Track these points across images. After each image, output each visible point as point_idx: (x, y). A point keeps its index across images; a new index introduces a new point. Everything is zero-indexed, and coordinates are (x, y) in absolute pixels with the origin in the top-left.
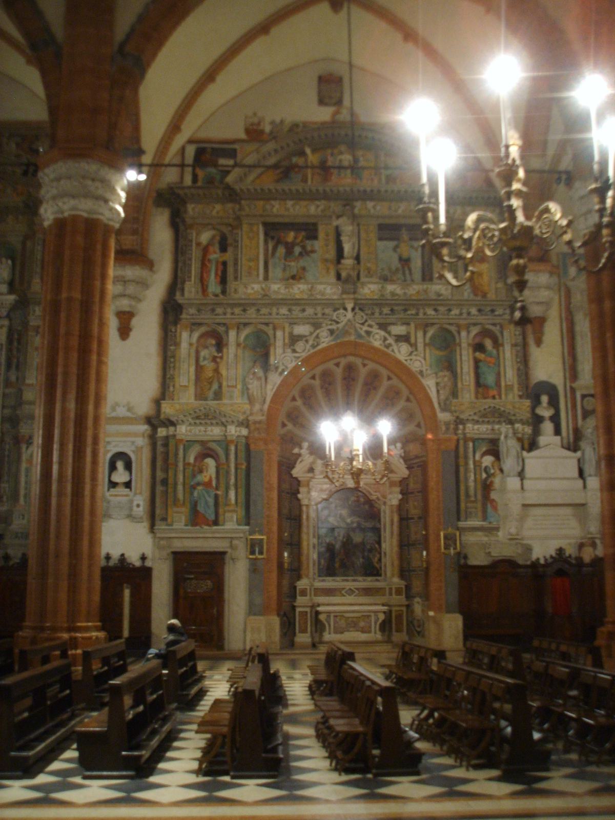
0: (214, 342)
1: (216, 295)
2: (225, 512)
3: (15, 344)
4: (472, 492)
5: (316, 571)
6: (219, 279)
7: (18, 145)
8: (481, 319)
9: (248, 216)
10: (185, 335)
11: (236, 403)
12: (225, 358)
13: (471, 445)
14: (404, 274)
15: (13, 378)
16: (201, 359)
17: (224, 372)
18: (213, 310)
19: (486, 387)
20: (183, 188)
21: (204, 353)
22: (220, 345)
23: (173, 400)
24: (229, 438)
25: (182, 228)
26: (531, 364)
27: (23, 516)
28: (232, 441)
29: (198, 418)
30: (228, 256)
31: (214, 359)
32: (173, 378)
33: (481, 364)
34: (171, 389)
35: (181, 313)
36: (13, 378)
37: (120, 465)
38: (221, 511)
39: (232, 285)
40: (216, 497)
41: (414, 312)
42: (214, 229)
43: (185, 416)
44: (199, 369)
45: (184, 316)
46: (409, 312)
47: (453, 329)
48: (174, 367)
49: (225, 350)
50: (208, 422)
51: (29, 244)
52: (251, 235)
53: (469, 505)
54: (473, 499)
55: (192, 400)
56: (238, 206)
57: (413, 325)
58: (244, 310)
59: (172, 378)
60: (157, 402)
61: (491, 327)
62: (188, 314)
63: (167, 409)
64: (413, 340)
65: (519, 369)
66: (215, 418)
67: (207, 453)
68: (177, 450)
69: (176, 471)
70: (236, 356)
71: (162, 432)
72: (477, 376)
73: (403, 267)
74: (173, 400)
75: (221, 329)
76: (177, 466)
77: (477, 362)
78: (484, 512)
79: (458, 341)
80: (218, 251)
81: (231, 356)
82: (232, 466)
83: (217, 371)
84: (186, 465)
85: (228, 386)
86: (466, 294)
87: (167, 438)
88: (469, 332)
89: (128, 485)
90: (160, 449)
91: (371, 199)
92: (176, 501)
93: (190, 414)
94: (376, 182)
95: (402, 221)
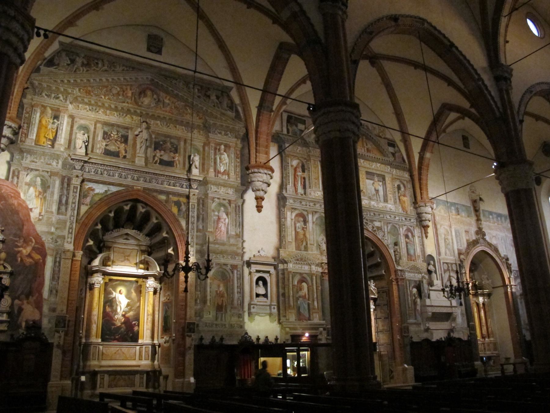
0: (302, 219)
1: (302, 195)
2: (313, 313)
3: (201, 206)
4: (410, 306)
6: (302, 186)
7: (198, 90)
8: (407, 223)
9: (312, 156)
10: (289, 214)
11: (314, 254)
12: (308, 228)
14: (377, 197)
15: (201, 227)
16: (297, 228)
17: (308, 236)
18: (301, 203)
19: (411, 256)
20: (283, 134)
21: (298, 225)
22: (305, 222)
23: (285, 249)
24: (312, 272)
25: (284, 155)
26: (425, 246)
27: (210, 312)
28: (314, 274)
29: (298, 260)
30: (306, 175)
31: (303, 229)
32: (285, 237)
33: (408, 244)
34: (284, 243)
35: (286, 202)
36: (201, 227)
37: (261, 283)
38: (311, 313)
39: (308, 190)
40: (309, 305)
42: (298, 159)
43: (291, 258)
44: (297, 233)
45: (287, 203)
47: (397, 226)
48: (285, 230)
49: (307, 225)
50: (303, 263)
51: (207, 148)
52: (315, 166)
53: (410, 312)
55: (294, 250)
56: (308, 150)
58: (315, 204)
59: (284, 236)
60: (278, 249)
61: (410, 227)
62: (289, 202)
63: (283, 253)
64: (383, 230)
65: (421, 248)
66: (305, 261)
67: (302, 280)
68: (289, 277)
69: (289, 290)
70: (313, 228)
71: (281, 266)
72: (407, 249)
74: (285, 249)
75: (305, 213)
76: (289, 286)
77: (407, 243)
78: (415, 315)
80: (301, 171)
81: (311, 228)
82: (315, 287)
83: (304, 235)
85: (311, 244)
86: (400, 210)
87: (283, 270)
88: (403, 229)
89: (265, 296)
90: (280, 276)
91: (363, 159)
92: (290, 306)
93: (294, 257)
94: (363, 150)
95: (375, 172)
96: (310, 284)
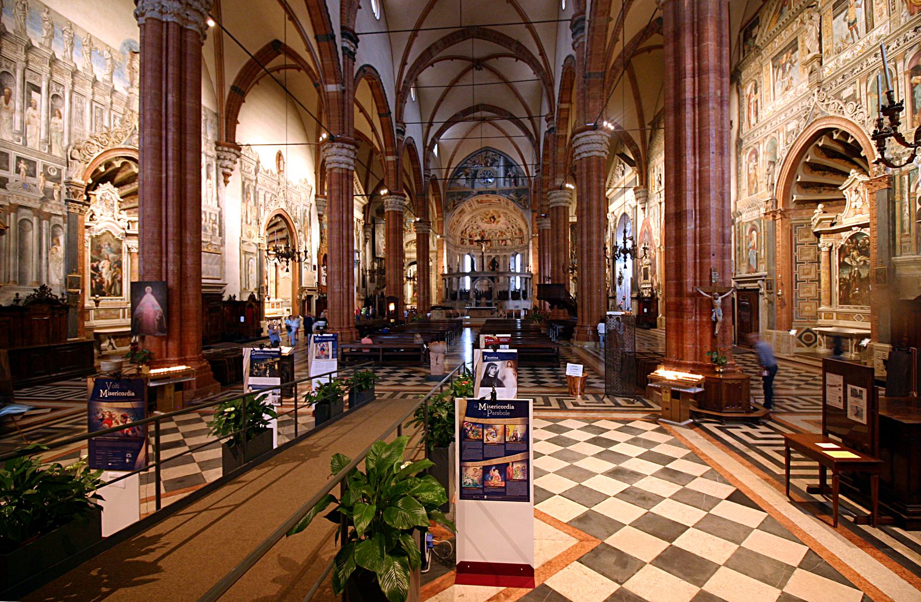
4: (906, 227)
5: (838, 300)
13: (906, 177)
14: (853, 37)
29: (749, 207)
41: (859, 69)
46: (855, 71)
53: (903, 239)
54: (907, 233)
57: (858, 82)
64: (858, 97)
73: (851, 30)
79: (894, 76)
84: (746, 237)
86: (903, 20)
96: (759, 231)
